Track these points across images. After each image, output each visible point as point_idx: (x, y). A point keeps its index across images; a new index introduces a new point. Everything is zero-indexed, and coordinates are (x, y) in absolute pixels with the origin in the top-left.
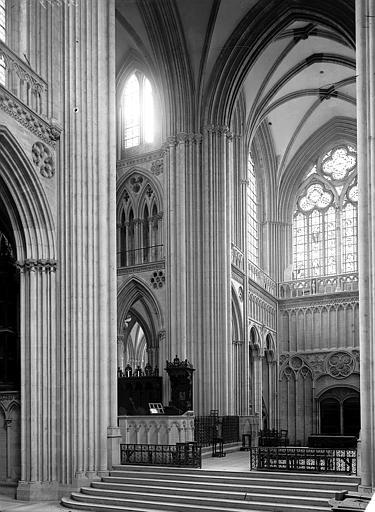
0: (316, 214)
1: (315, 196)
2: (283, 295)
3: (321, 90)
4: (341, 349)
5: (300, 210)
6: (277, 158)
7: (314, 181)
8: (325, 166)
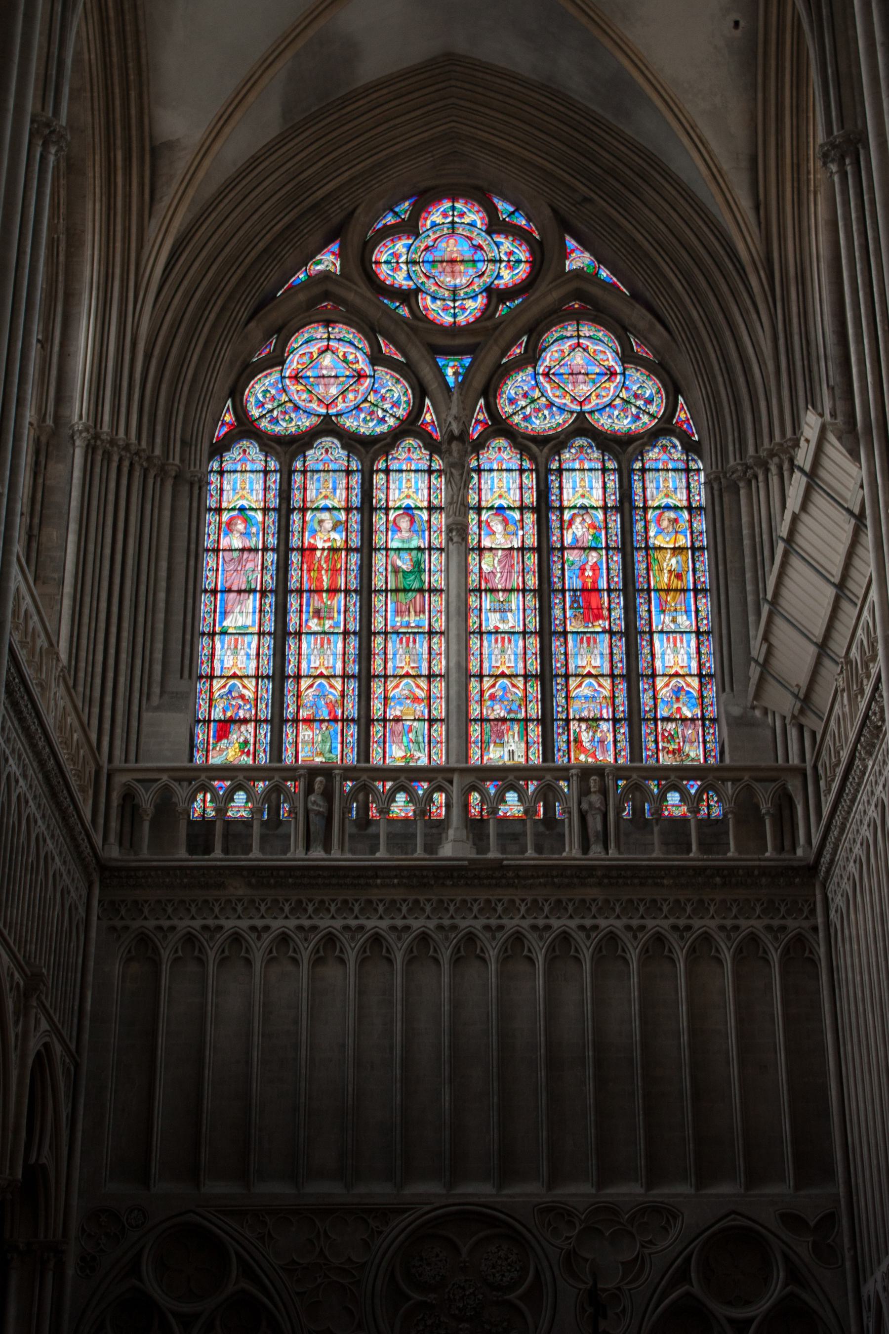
0: (328, 454)
4: (479, 1190)
5: (246, 429)
7: (326, 303)
8: (382, 254)
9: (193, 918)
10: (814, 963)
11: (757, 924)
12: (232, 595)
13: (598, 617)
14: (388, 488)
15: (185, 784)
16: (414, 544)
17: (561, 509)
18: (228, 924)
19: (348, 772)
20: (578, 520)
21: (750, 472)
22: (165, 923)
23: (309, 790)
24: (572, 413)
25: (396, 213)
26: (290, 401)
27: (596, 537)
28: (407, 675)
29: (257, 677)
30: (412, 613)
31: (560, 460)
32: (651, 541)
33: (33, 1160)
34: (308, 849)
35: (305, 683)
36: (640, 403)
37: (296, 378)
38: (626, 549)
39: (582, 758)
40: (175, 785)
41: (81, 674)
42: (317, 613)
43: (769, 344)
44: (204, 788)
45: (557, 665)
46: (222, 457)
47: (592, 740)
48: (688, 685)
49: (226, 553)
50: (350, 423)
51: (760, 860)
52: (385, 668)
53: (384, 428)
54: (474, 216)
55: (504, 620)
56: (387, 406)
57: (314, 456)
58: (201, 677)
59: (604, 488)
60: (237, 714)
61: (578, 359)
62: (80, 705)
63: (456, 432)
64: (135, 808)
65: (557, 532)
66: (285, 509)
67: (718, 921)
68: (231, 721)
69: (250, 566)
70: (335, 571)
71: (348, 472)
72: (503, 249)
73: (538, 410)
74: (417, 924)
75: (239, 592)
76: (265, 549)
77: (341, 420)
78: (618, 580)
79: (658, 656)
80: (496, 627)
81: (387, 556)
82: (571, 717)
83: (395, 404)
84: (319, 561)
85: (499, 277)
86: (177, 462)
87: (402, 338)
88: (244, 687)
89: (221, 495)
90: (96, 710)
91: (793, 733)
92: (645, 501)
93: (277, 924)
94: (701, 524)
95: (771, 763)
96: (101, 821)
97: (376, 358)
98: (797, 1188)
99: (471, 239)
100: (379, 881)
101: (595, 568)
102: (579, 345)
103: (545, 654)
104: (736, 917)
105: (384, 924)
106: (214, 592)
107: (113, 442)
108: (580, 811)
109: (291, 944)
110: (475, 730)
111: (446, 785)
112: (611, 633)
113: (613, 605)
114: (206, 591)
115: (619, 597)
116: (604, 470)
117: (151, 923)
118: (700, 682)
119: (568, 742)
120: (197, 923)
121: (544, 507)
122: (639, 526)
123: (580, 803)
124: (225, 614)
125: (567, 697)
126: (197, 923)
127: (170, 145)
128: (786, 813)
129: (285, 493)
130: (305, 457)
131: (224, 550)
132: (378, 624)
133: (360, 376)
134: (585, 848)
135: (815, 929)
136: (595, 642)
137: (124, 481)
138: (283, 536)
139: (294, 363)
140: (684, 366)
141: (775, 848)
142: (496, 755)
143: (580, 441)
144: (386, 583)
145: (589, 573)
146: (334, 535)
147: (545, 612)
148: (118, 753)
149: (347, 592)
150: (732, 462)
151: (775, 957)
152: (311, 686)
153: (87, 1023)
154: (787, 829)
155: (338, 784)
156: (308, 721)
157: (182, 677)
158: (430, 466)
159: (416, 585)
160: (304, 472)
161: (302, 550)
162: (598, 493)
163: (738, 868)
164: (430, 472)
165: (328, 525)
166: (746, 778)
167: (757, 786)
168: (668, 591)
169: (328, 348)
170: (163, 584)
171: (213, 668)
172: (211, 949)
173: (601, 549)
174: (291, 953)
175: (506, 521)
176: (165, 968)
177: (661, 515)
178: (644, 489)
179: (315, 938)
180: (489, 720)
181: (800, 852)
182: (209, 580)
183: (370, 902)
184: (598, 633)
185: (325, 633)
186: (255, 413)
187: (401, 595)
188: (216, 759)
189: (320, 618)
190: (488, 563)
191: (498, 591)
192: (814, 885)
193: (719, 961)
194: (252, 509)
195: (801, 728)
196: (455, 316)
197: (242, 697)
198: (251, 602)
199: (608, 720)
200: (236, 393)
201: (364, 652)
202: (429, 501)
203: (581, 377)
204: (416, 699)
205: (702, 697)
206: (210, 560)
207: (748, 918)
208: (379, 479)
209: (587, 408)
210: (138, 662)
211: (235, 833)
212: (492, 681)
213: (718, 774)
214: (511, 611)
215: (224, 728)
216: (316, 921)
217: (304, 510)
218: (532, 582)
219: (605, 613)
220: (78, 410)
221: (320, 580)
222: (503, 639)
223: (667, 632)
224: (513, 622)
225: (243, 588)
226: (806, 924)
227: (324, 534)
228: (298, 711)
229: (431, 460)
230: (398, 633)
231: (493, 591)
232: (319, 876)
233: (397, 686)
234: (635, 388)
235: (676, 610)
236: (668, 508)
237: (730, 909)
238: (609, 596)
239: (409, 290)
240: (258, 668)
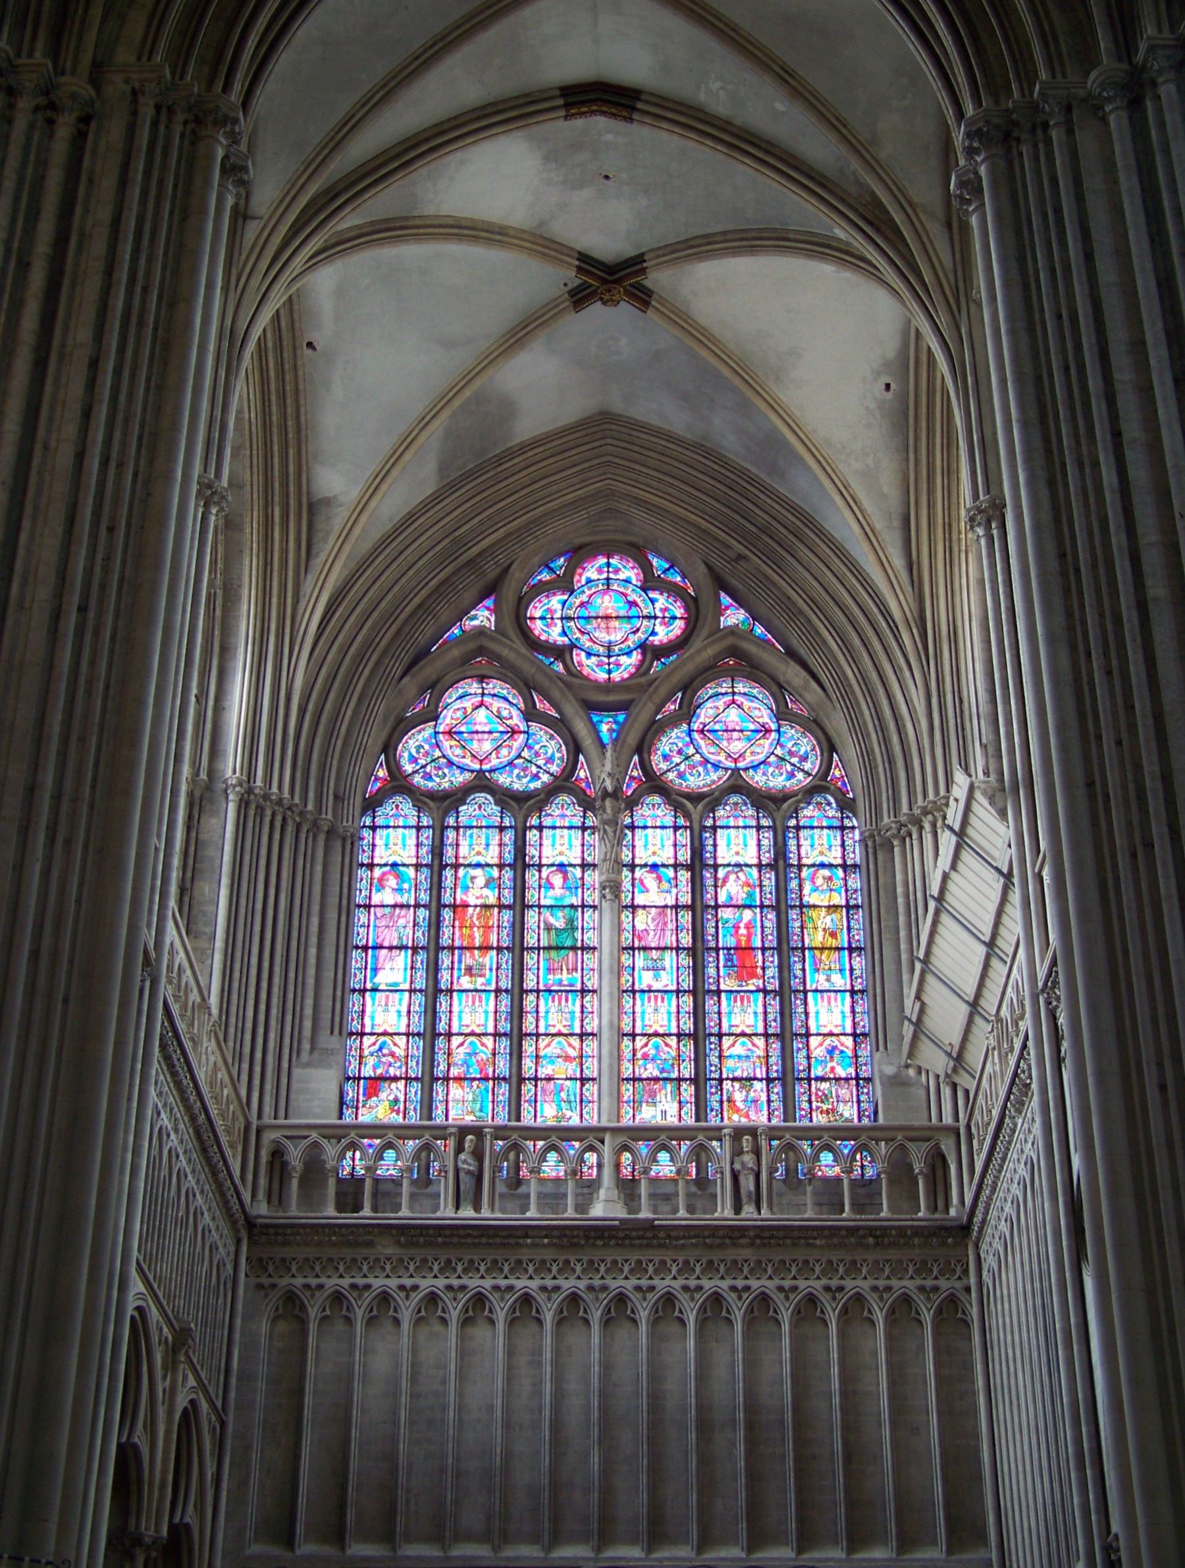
0: (480, 809)
1: (479, 726)
2: (277, 1196)
3: (579, 253)
5: (399, 784)
6: (314, 508)
7: (480, 659)
8: (536, 610)
9: (341, 1276)
10: (967, 1325)
11: (909, 1285)
12: (384, 952)
13: (753, 975)
14: (541, 845)
15: (334, 1141)
16: (567, 902)
17: (716, 867)
18: (377, 1283)
19: (500, 1132)
20: (732, 877)
21: (904, 830)
22: (314, 1282)
23: (460, 1149)
24: (727, 769)
25: (551, 569)
26: (444, 756)
27: (750, 895)
28: (559, 1034)
29: (407, 1035)
30: (565, 971)
31: (714, 818)
32: (806, 899)
33: (177, 1520)
34: (457, 1208)
35: (456, 1041)
36: (795, 760)
37: (450, 733)
38: (781, 906)
39: (735, 1117)
40: (324, 1142)
41: (232, 1030)
42: (469, 971)
43: (923, 700)
44: (353, 1146)
45: (711, 1024)
46: (374, 812)
47: (745, 1101)
48: (842, 1045)
49: (378, 909)
50: (503, 779)
51: (913, 1220)
52: (537, 1027)
53: (537, 784)
54: (629, 572)
55: (656, 978)
56: (541, 762)
57: (467, 812)
58: (351, 1034)
59: (759, 845)
60: (387, 1071)
61: (733, 715)
62: (230, 1060)
63: (610, 789)
64: (284, 1165)
65: (711, 890)
66: (438, 864)
67: (870, 1282)
68: (382, 1078)
69: (402, 922)
70: (487, 928)
71: (502, 829)
72: (658, 605)
73: (692, 767)
74: (568, 1284)
75: (391, 948)
76: (417, 906)
77: (495, 776)
78: (771, 941)
79: (812, 1015)
80: (649, 986)
81: (540, 913)
82: (724, 1076)
83: (550, 760)
84: (472, 917)
85: (653, 633)
86: (330, 816)
87: (556, 694)
88: (395, 1044)
89: (373, 851)
90: (245, 1066)
91: (946, 1092)
92: (800, 858)
93: (426, 1284)
94: (855, 882)
95: (925, 1122)
96: (250, 1177)
97: (530, 714)
98: (950, 1552)
99: (625, 595)
100: (529, 1241)
101: (748, 926)
102: (733, 702)
103: (698, 1013)
104: (888, 1278)
105: (534, 1284)
106: (365, 948)
107: (266, 797)
108: (732, 1170)
109: (440, 1304)
110: (627, 1090)
111: (598, 1144)
112: (765, 992)
113: (767, 964)
114: (357, 947)
115: (772, 956)
116: (759, 828)
117: (299, 1281)
118: (855, 1041)
119: (721, 1102)
120: (346, 1282)
121: (699, 864)
122: (794, 884)
123: (732, 1163)
124: (376, 970)
125: (720, 1057)
126: (346, 1282)
127: (327, 502)
128: (939, 1173)
129: (438, 850)
130: (458, 812)
131: (376, 906)
132: (530, 982)
133: (514, 732)
134: (738, 1209)
135: (968, 1290)
136: (749, 1001)
137: (277, 836)
138: (435, 892)
139: (448, 718)
140: (838, 723)
141: (928, 1208)
142: (648, 1115)
143: (734, 799)
144: (539, 940)
145: (743, 931)
146: (486, 892)
147: (698, 970)
148: (268, 1109)
149: (499, 949)
150: (886, 820)
151: (927, 1317)
152: (462, 1044)
153: (233, 1381)
154: (940, 1188)
155: (488, 1143)
156: (458, 1079)
157: (332, 1033)
158: (584, 823)
159: (569, 943)
160: (457, 828)
161: (454, 907)
162: (752, 850)
163: (891, 1228)
164: (584, 828)
165: (481, 881)
166: (899, 1138)
167: (909, 1145)
168: (822, 949)
169: (482, 704)
170: (314, 940)
171: (363, 1025)
172: (359, 1307)
173: (756, 907)
174: (439, 1313)
175: (659, 878)
176: (313, 1327)
177: (815, 873)
178: (799, 846)
179: (464, 1298)
180: (641, 1080)
181: (953, 1212)
182: (360, 936)
183: (519, 1262)
184: (752, 992)
185: (477, 991)
186: (408, 768)
187: (553, 953)
188: (365, 1117)
189: (471, 975)
190: (643, 920)
191: (651, 949)
192: (967, 1246)
193: (872, 1323)
194: (404, 865)
195: (954, 1087)
196: (609, 672)
197: (392, 1054)
198: (402, 959)
199: (761, 1080)
200: (389, 748)
201: (516, 1010)
202: (583, 859)
203: (735, 735)
204: (568, 1058)
205: (856, 1056)
206: (361, 916)
207: (900, 1279)
208: (532, 836)
209: (741, 765)
210: (289, 1018)
211: (385, 1192)
212: (645, 1040)
213: (871, 1134)
214: (664, 969)
215: (375, 1084)
216: (465, 1281)
217: (456, 866)
218: (686, 940)
219: (759, 971)
220: (231, 765)
221: (472, 937)
222: (656, 998)
223: (822, 991)
224: (667, 980)
225: (395, 943)
226: (958, 1285)
227: (476, 890)
228: (449, 1069)
229: (584, 817)
230: (550, 991)
231: (646, 949)
232: (469, 1235)
233: (549, 1045)
234: (789, 745)
235: (830, 969)
236: (822, 865)
237: (883, 1270)
238: (763, 955)
239: (564, 645)
240: (408, 1026)
